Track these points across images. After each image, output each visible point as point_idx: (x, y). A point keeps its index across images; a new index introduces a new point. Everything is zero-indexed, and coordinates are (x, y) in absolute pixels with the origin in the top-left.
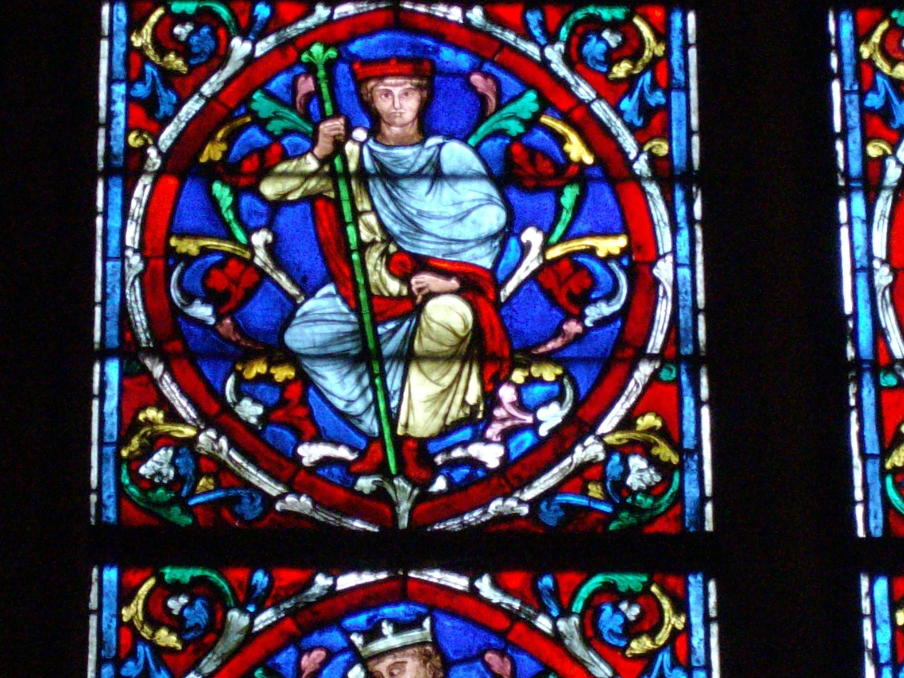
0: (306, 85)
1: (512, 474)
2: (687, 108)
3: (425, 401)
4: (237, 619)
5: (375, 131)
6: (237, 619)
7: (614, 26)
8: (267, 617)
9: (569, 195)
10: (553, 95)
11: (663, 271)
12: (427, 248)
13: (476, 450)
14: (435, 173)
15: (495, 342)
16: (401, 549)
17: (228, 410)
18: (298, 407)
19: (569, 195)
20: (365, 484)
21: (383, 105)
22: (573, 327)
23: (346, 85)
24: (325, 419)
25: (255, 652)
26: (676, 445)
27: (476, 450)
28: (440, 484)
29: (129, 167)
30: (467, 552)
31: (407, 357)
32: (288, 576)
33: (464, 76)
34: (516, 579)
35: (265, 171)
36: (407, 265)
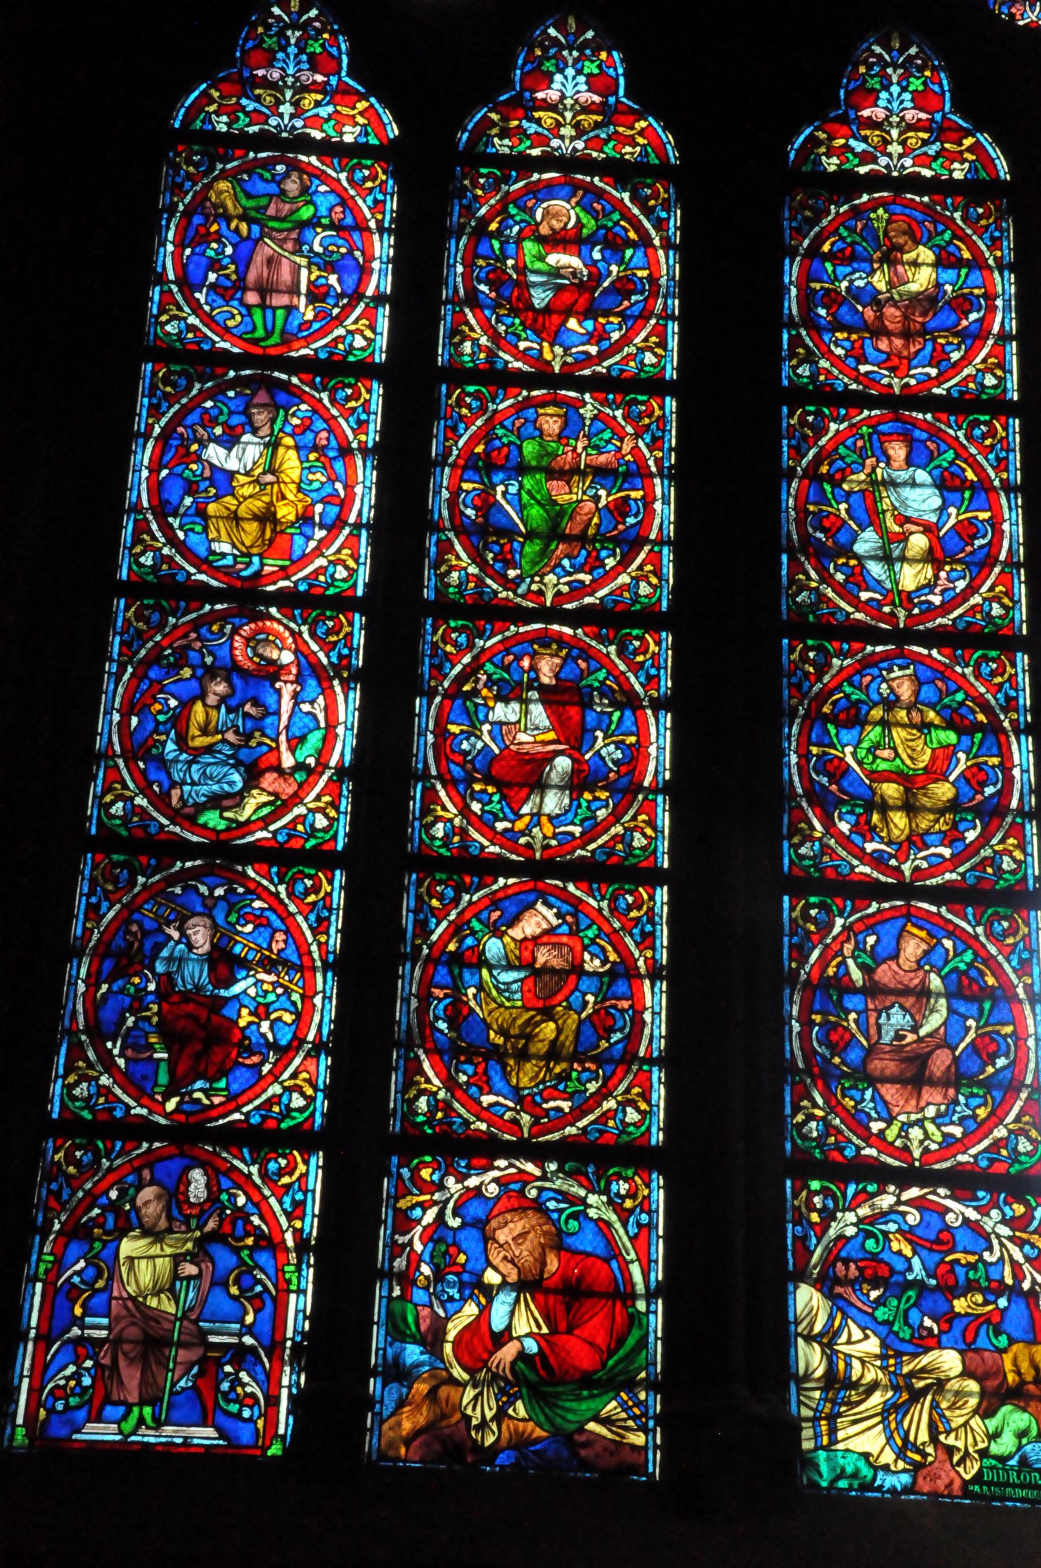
0: (860, 443)
1: (946, 608)
2: (1016, 459)
3: (910, 577)
4: (836, 662)
5: (888, 464)
6: (836, 662)
7: (985, 423)
8: (847, 662)
9: (967, 494)
10: (961, 453)
11: (1006, 526)
12: (910, 513)
13: (931, 598)
14: (914, 484)
15: (939, 554)
16: (902, 637)
17: (832, 576)
18: (858, 578)
19: (967, 494)
20: (887, 609)
21: (891, 452)
22: (969, 549)
23: (877, 444)
24: (872, 583)
25: (844, 675)
26: (1011, 599)
27: (931, 598)
28: (916, 611)
29: (791, 473)
30: (929, 639)
31: (903, 559)
32: (856, 646)
33: (924, 442)
34: (947, 651)
35: (843, 480)
36: (903, 520)
